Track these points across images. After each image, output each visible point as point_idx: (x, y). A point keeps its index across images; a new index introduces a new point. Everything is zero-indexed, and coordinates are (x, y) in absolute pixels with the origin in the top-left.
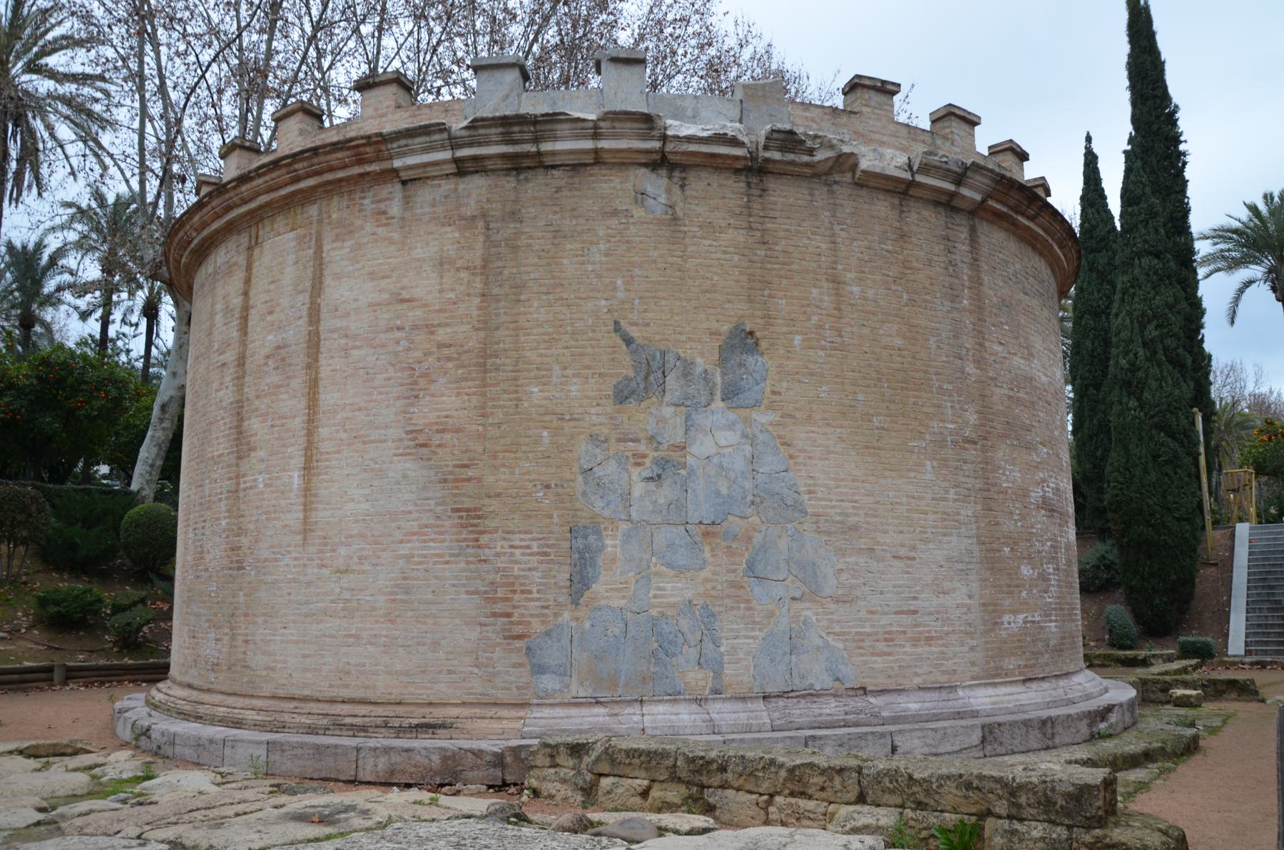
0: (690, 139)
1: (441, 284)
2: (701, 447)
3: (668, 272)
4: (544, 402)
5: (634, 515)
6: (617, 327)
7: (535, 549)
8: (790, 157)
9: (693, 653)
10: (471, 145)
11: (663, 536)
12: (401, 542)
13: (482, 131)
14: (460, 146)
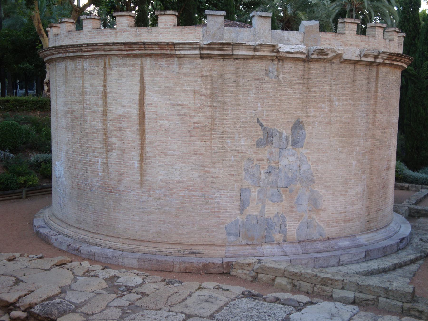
0: (287, 53)
1: (195, 100)
2: (284, 162)
3: (276, 101)
4: (232, 146)
5: (262, 185)
6: (258, 121)
7: (229, 195)
8: (321, 57)
9: (278, 229)
10: (208, 50)
11: (271, 191)
12: (181, 191)
13: (212, 46)
14: (203, 50)
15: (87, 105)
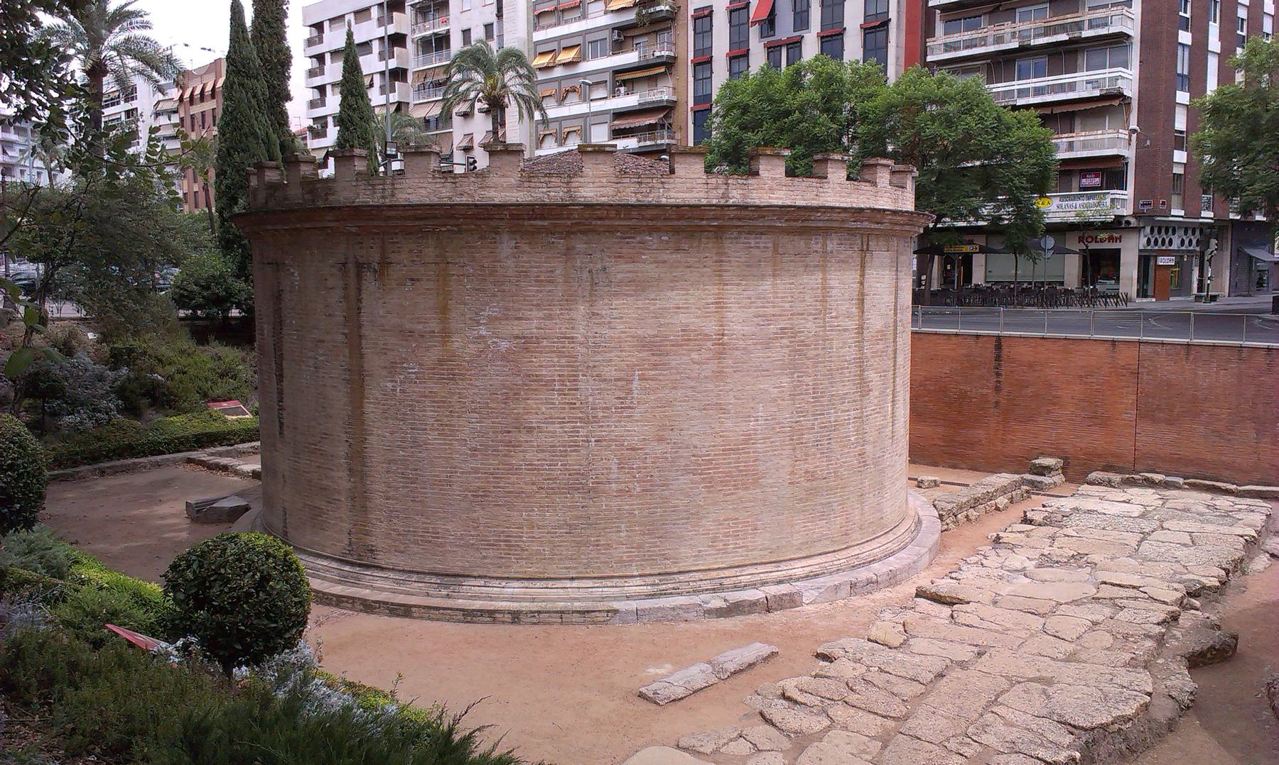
15: (831, 317)
